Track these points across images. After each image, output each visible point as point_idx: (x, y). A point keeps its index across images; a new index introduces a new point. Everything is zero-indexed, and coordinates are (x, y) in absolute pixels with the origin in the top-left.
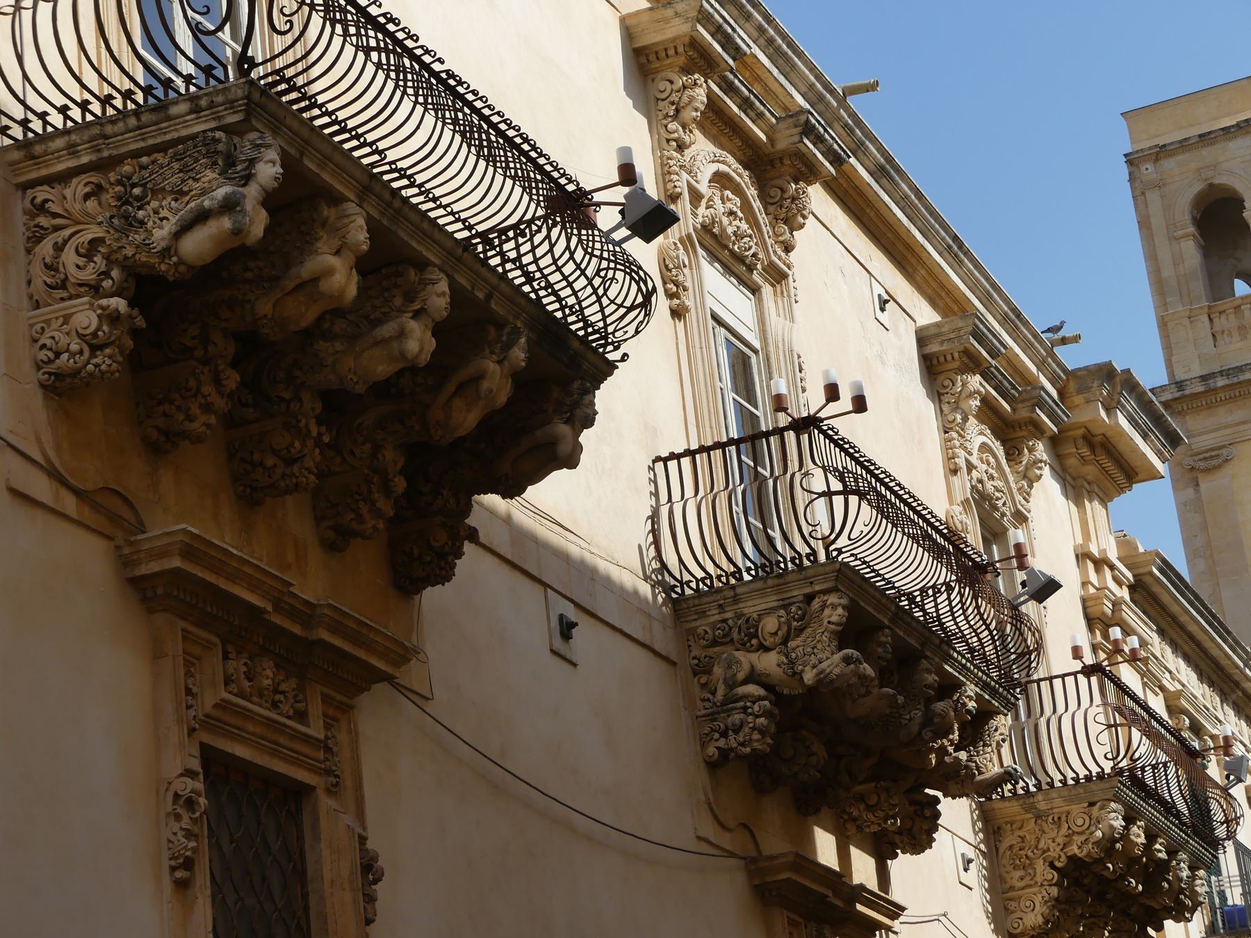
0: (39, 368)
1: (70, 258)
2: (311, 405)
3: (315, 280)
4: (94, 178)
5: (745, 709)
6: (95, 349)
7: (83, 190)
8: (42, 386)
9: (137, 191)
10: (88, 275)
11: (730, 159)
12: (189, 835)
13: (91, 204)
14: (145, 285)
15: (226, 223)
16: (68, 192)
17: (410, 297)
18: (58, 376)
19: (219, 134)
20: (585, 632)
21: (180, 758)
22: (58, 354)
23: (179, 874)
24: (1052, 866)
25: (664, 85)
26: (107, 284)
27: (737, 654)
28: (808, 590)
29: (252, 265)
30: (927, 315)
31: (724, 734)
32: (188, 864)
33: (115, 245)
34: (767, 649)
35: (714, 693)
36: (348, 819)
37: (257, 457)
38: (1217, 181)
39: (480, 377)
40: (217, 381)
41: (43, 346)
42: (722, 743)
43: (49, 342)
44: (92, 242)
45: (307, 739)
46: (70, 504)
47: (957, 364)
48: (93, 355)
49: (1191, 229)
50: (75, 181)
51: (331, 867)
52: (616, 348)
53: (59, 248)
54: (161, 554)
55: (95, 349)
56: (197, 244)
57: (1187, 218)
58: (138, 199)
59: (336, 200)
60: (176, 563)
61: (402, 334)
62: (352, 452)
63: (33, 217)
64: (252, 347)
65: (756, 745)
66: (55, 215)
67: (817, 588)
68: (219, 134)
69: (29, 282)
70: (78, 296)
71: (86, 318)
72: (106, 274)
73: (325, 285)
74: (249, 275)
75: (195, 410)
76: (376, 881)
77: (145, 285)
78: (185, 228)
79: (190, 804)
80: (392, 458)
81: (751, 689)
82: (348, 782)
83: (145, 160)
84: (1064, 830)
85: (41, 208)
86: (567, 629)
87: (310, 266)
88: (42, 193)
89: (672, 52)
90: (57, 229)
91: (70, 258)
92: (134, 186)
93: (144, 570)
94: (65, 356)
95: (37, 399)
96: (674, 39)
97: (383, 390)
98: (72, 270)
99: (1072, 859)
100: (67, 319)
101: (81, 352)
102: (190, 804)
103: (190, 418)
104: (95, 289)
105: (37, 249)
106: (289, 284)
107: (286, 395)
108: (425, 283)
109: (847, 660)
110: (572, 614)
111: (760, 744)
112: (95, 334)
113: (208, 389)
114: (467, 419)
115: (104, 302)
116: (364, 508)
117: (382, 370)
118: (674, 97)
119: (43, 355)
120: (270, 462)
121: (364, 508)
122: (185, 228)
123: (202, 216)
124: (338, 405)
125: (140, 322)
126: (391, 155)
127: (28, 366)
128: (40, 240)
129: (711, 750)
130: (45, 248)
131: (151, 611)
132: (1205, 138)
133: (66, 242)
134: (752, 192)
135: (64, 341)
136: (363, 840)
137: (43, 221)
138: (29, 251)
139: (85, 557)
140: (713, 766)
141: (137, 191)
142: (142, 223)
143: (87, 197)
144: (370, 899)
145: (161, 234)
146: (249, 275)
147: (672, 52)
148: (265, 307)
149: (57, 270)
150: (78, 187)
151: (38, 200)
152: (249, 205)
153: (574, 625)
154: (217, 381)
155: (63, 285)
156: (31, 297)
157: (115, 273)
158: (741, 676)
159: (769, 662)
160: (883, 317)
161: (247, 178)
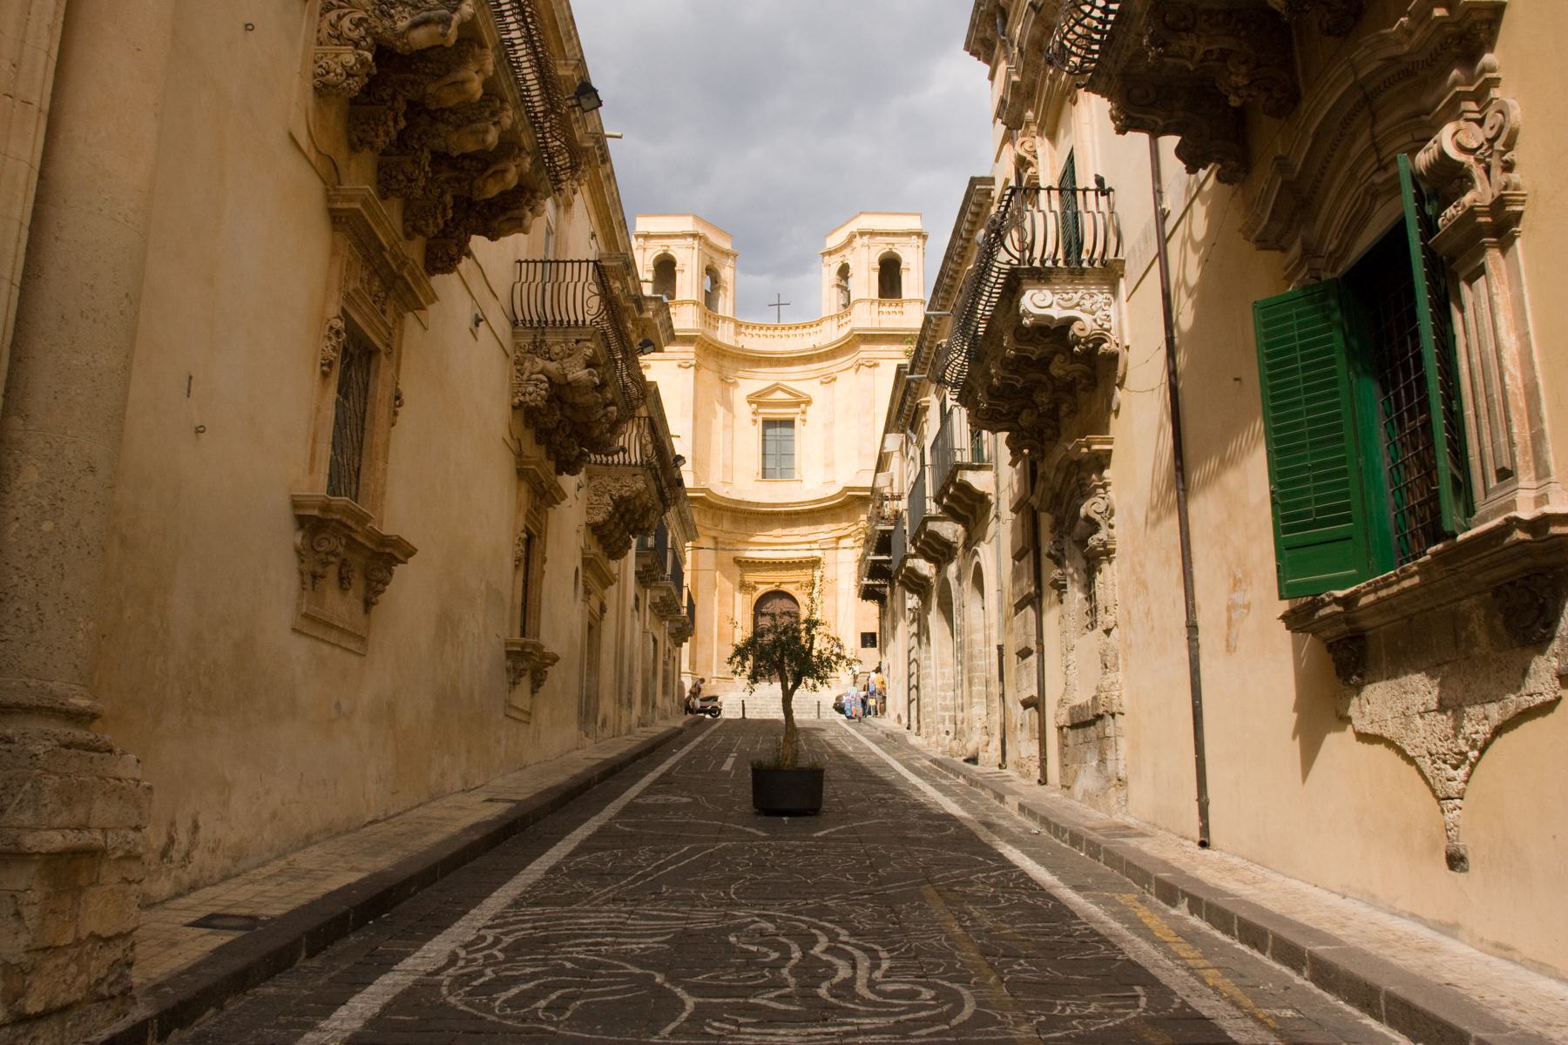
1: (346, 23)
2: (426, 157)
3: (463, 82)
6: (349, 75)
10: (355, 35)
12: (334, 349)
14: (384, 53)
15: (440, 29)
17: (493, 114)
18: (325, 85)
21: (333, 310)
32: (330, 365)
36: (393, 371)
39: (504, 171)
40: (396, 122)
45: (385, 324)
46: (313, 156)
51: (381, 392)
53: (340, 18)
54: (351, 199)
55: (349, 75)
56: (421, 37)
59: (482, 46)
60: (358, 206)
61: (486, 131)
64: (416, 109)
71: (349, 58)
72: (364, 38)
73: (467, 86)
75: (381, 132)
77: (384, 53)
78: (415, 25)
79: (338, 333)
80: (448, 198)
81: (541, 377)
86: (477, 321)
87: (462, 75)
91: (346, 23)
93: (339, 206)
95: (311, 94)
99: (621, 497)
100: (337, 55)
102: (338, 333)
104: (357, 45)
106: (449, 80)
108: (503, 109)
109: (590, 373)
111: (541, 404)
113: (391, 124)
114: (493, 190)
116: (431, 221)
117: (471, 147)
120: (401, 177)
121: (431, 221)
122: (415, 25)
123: (426, 22)
124: (440, 158)
125: (375, 71)
127: (310, 75)
130: (333, 16)
131: (334, 230)
132: (669, 236)
135: (333, 66)
139: (313, 189)
140: (514, 408)
142: (391, 16)
144: (396, 414)
145: (402, 24)
148: (431, 89)
152: (453, 24)
154: (396, 122)
159: (552, 366)
161: (455, 10)
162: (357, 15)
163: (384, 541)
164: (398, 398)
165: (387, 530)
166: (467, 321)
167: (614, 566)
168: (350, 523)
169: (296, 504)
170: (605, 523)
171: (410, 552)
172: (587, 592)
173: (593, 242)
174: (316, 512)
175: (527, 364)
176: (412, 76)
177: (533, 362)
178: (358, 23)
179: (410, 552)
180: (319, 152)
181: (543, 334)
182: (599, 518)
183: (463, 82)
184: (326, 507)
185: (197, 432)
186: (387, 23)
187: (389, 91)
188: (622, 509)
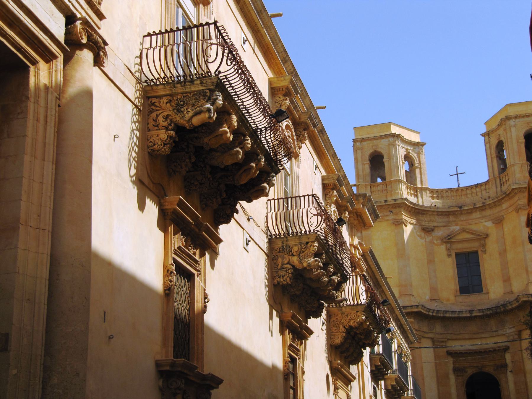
0: (148, 148)
1: (161, 118)
3: (222, 135)
4: (170, 98)
5: (286, 271)
7: (166, 101)
8: (149, 153)
9: (182, 103)
10: (165, 124)
11: (290, 122)
13: (168, 105)
16: (161, 101)
18: (153, 151)
19: (207, 91)
20: (251, 243)
22: (154, 145)
23: (167, 292)
24: (344, 327)
25: (278, 98)
26: (170, 127)
27: (285, 256)
28: (307, 241)
29: (204, 128)
30: (324, 174)
31: (279, 277)
33: (174, 117)
34: (294, 256)
35: (278, 266)
36: (202, 284)
37: (192, 182)
38: (377, 150)
41: (151, 142)
42: (278, 279)
43: (152, 141)
44: (167, 115)
46: (151, 186)
47: (331, 187)
48: (164, 146)
49: (368, 162)
50: (164, 98)
52: (282, 166)
53: (157, 116)
55: (165, 144)
57: (368, 159)
58: (182, 105)
62: (213, 184)
63: (150, 106)
64: (199, 151)
65: (288, 281)
66: (157, 106)
67: (310, 240)
68: (207, 91)
69: (148, 124)
70: (162, 129)
73: (224, 136)
74: (203, 131)
76: (208, 302)
77: (179, 129)
81: (288, 266)
82: (202, 274)
83: (185, 95)
84: (349, 318)
85: (153, 104)
88: (154, 100)
89: (281, 90)
90: (157, 110)
91: (161, 118)
92: (181, 101)
94: (157, 145)
95: (147, 156)
96: (282, 86)
97: (226, 169)
98: (161, 122)
99: (351, 327)
101: (161, 145)
103: (181, 168)
104: (167, 129)
105: (151, 115)
107: (203, 166)
110: (249, 239)
112: (166, 141)
113: (188, 160)
115: (169, 132)
118: (280, 102)
119: (150, 144)
124: (214, 169)
126: (245, 103)
128: (152, 113)
129: (276, 281)
130: (154, 115)
132: (376, 138)
133: (159, 114)
134: (293, 131)
136: (205, 290)
137: (153, 107)
138: (148, 115)
141: (182, 103)
142: (183, 112)
143: (167, 103)
145: (187, 116)
146: (203, 131)
147: (281, 90)
149: (156, 121)
150: (165, 100)
151: (153, 102)
153: (249, 241)
154: (190, 158)
155: (157, 126)
156: (148, 128)
157: (172, 125)
158: (286, 262)
159: (295, 260)
160: (316, 171)
162: (166, 114)
163: (205, 377)
164: (206, 298)
165: (206, 372)
166: (241, 243)
167: (354, 369)
168: (186, 372)
169: (158, 364)
170: (342, 344)
171: (220, 381)
172: (336, 389)
173: (317, 171)
174: (168, 368)
175: (280, 260)
176: (196, 135)
177: (283, 258)
178: (166, 118)
179: (220, 381)
180: (153, 183)
181: (287, 241)
182: (338, 341)
183: (222, 135)
184: (173, 364)
185: (110, 338)
186: (180, 115)
187: (186, 144)
188: (352, 333)
